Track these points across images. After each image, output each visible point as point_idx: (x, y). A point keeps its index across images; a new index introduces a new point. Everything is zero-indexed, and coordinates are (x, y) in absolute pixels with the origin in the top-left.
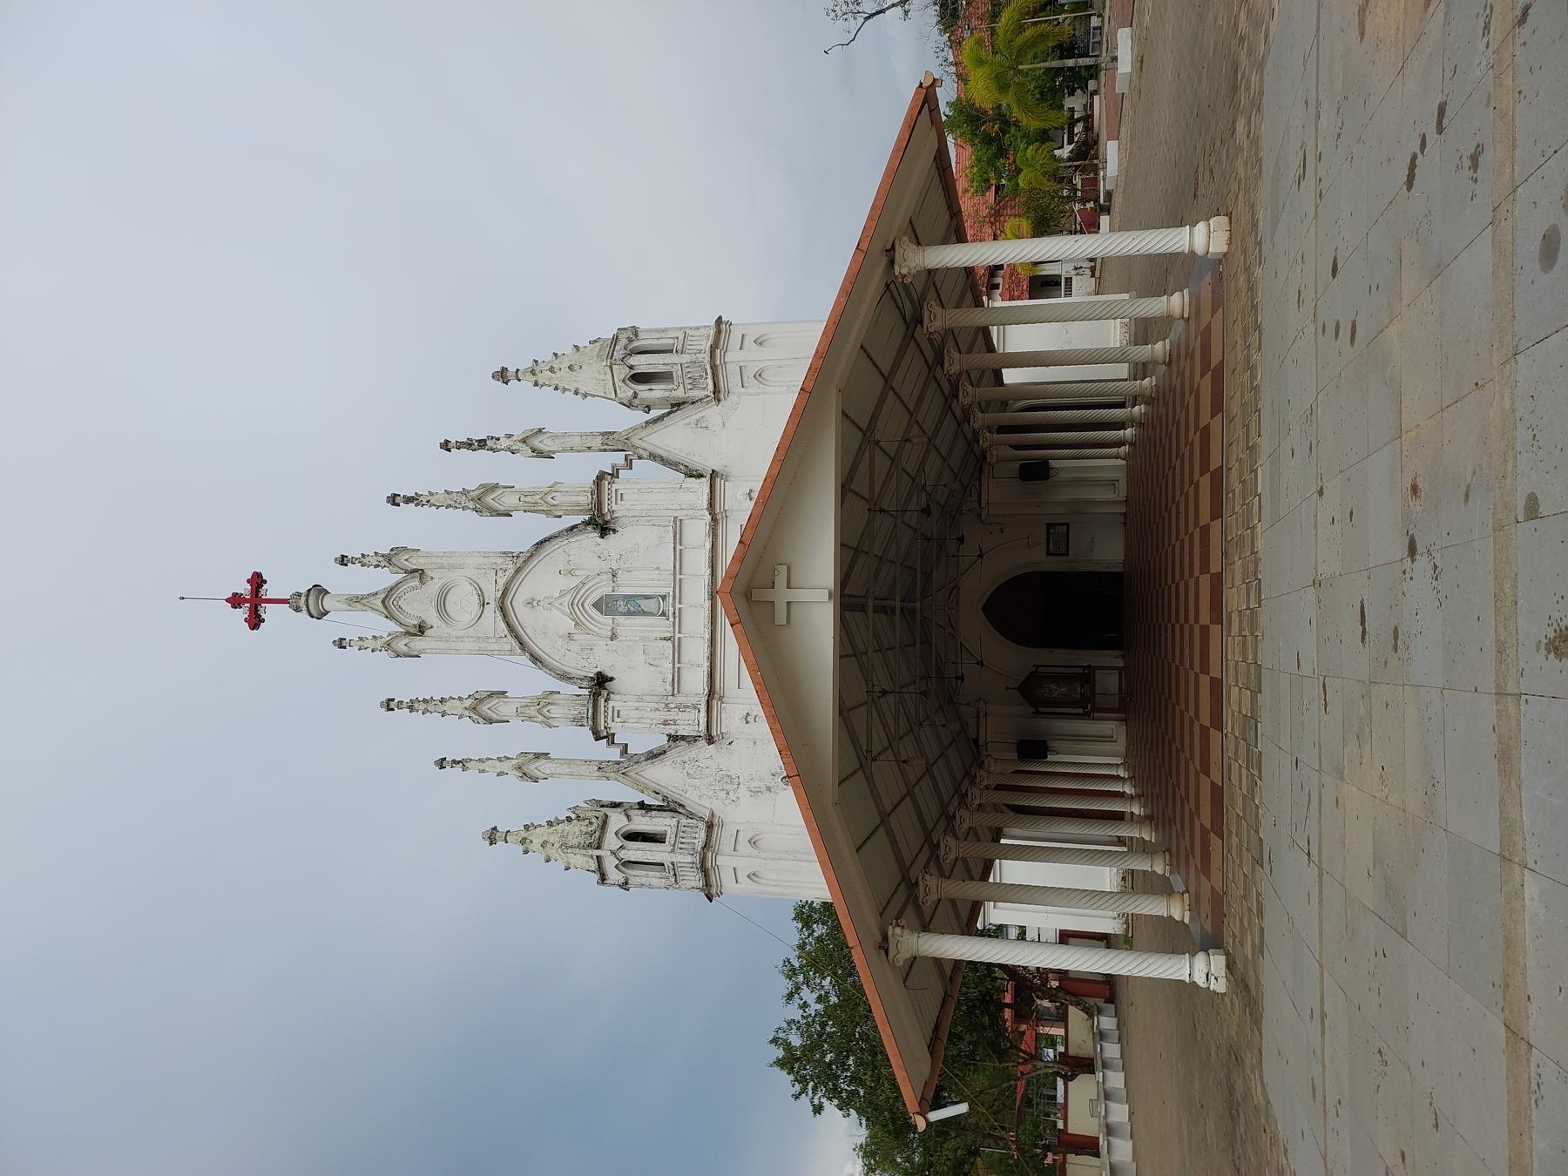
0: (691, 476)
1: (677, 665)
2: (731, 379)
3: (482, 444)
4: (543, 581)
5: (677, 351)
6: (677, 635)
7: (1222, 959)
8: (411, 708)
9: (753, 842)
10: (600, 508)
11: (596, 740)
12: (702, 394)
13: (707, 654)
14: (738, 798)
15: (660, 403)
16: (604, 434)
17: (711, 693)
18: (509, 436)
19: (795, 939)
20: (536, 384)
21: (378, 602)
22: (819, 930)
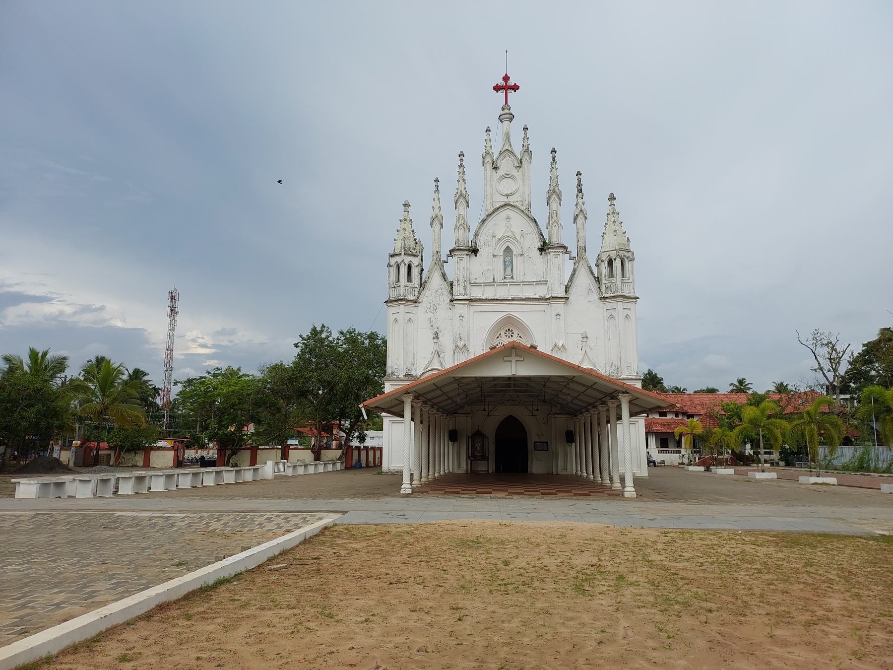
0: (566, 288)
1: (483, 284)
2: (610, 304)
3: (580, 191)
4: (519, 224)
5: (623, 280)
6: (496, 284)
7: (410, 492)
8: (461, 166)
9: (410, 320)
10: (550, 248)
11: (450, 251)
12: (604, 292)
13: (488, 298)
14: (427, 313)
15: (599, 272)
16: (585, 247)
17: (472, 300)
18: (584, 204)
19: (362, 332)
20: (608, 214)
21: (507, 148)
22: (367, 342)
